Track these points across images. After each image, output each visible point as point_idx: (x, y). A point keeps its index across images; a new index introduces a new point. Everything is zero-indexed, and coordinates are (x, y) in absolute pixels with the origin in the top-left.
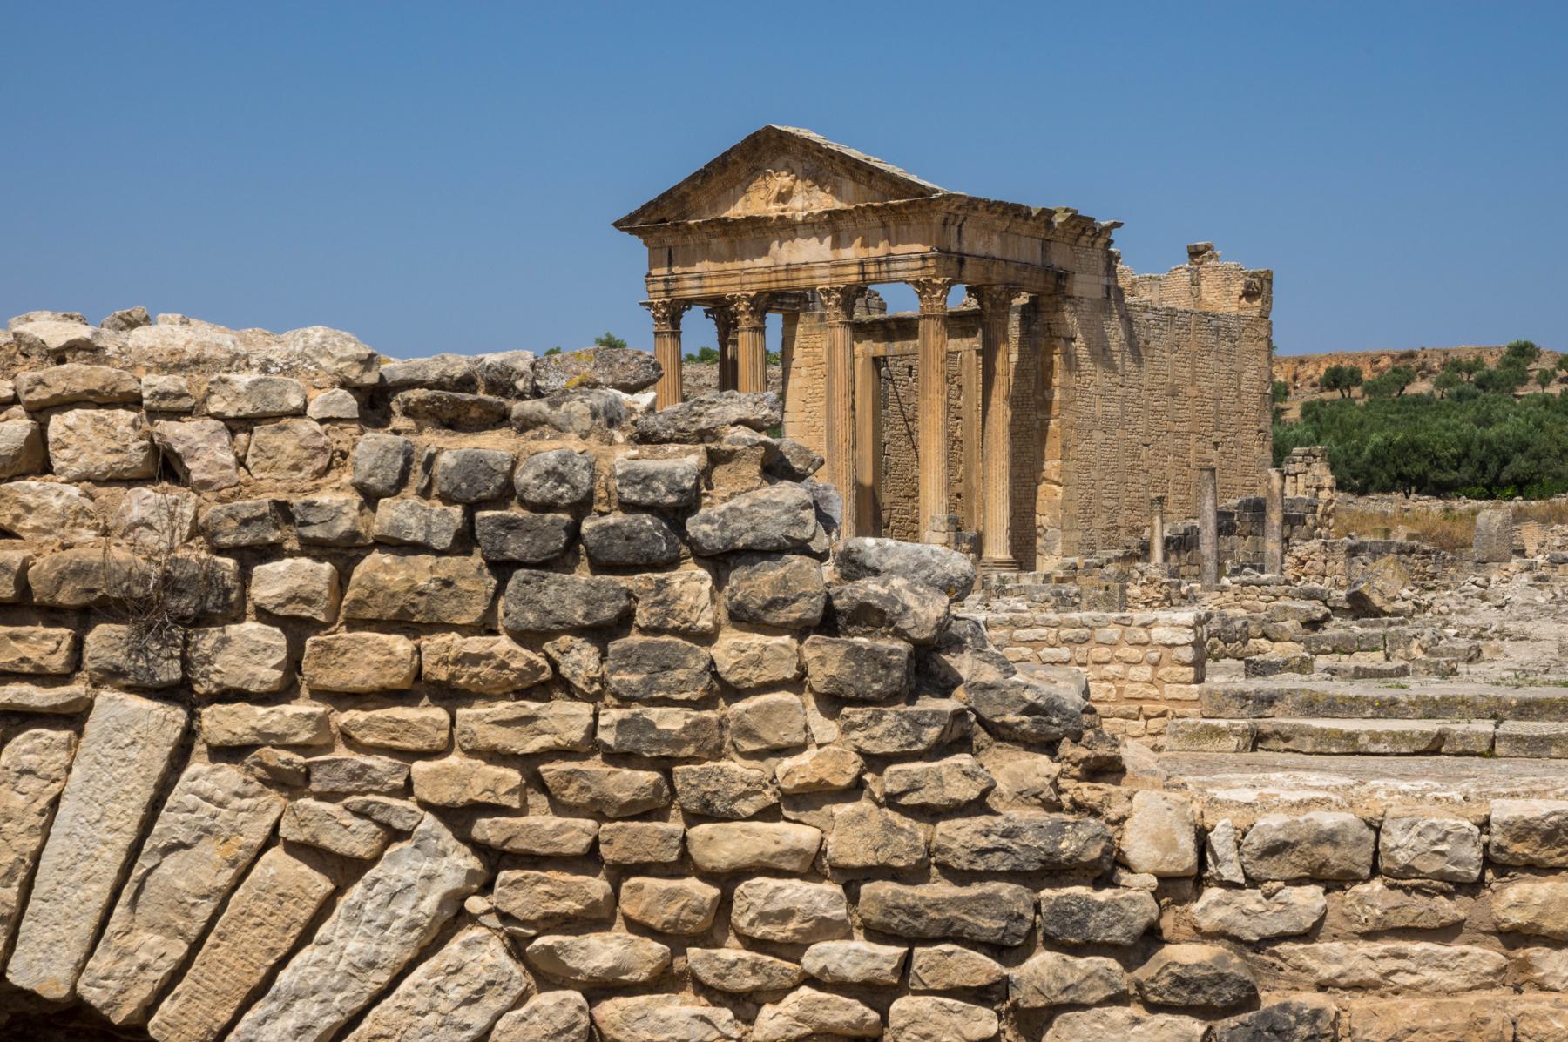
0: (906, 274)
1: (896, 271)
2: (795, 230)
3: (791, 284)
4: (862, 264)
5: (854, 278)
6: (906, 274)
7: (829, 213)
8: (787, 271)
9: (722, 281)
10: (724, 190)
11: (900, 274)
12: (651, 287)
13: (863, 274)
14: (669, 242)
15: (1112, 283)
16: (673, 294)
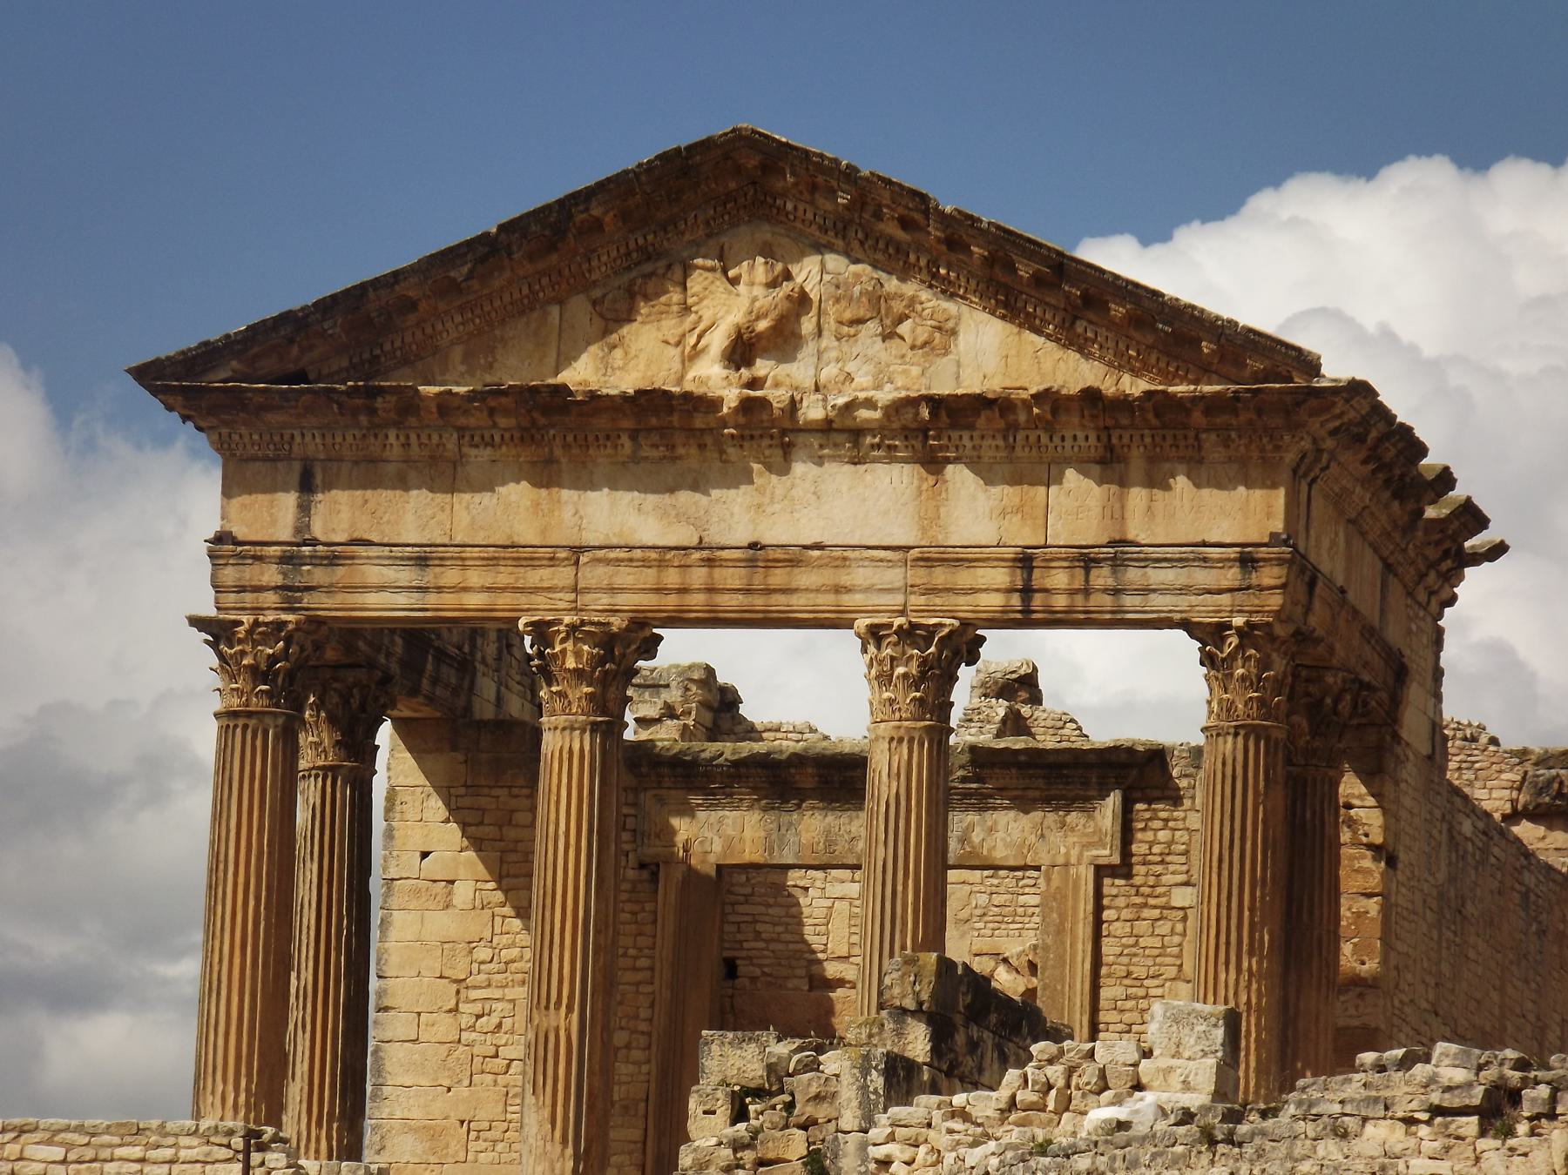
0: (1183, 602)
1: (1147, 591)
3: (758, 601)
4: (1025, 561)
5: (993, 601)
6: (1183, 602)
7: (935, 402)
8: (751, 563)
9: (504, 577)
10: (529, 305)
11: (1160, 603)
12: (230, 575)
13: (1027, 591)
14: (313, 445)
15: (1437, 720)
16: (308, 600)
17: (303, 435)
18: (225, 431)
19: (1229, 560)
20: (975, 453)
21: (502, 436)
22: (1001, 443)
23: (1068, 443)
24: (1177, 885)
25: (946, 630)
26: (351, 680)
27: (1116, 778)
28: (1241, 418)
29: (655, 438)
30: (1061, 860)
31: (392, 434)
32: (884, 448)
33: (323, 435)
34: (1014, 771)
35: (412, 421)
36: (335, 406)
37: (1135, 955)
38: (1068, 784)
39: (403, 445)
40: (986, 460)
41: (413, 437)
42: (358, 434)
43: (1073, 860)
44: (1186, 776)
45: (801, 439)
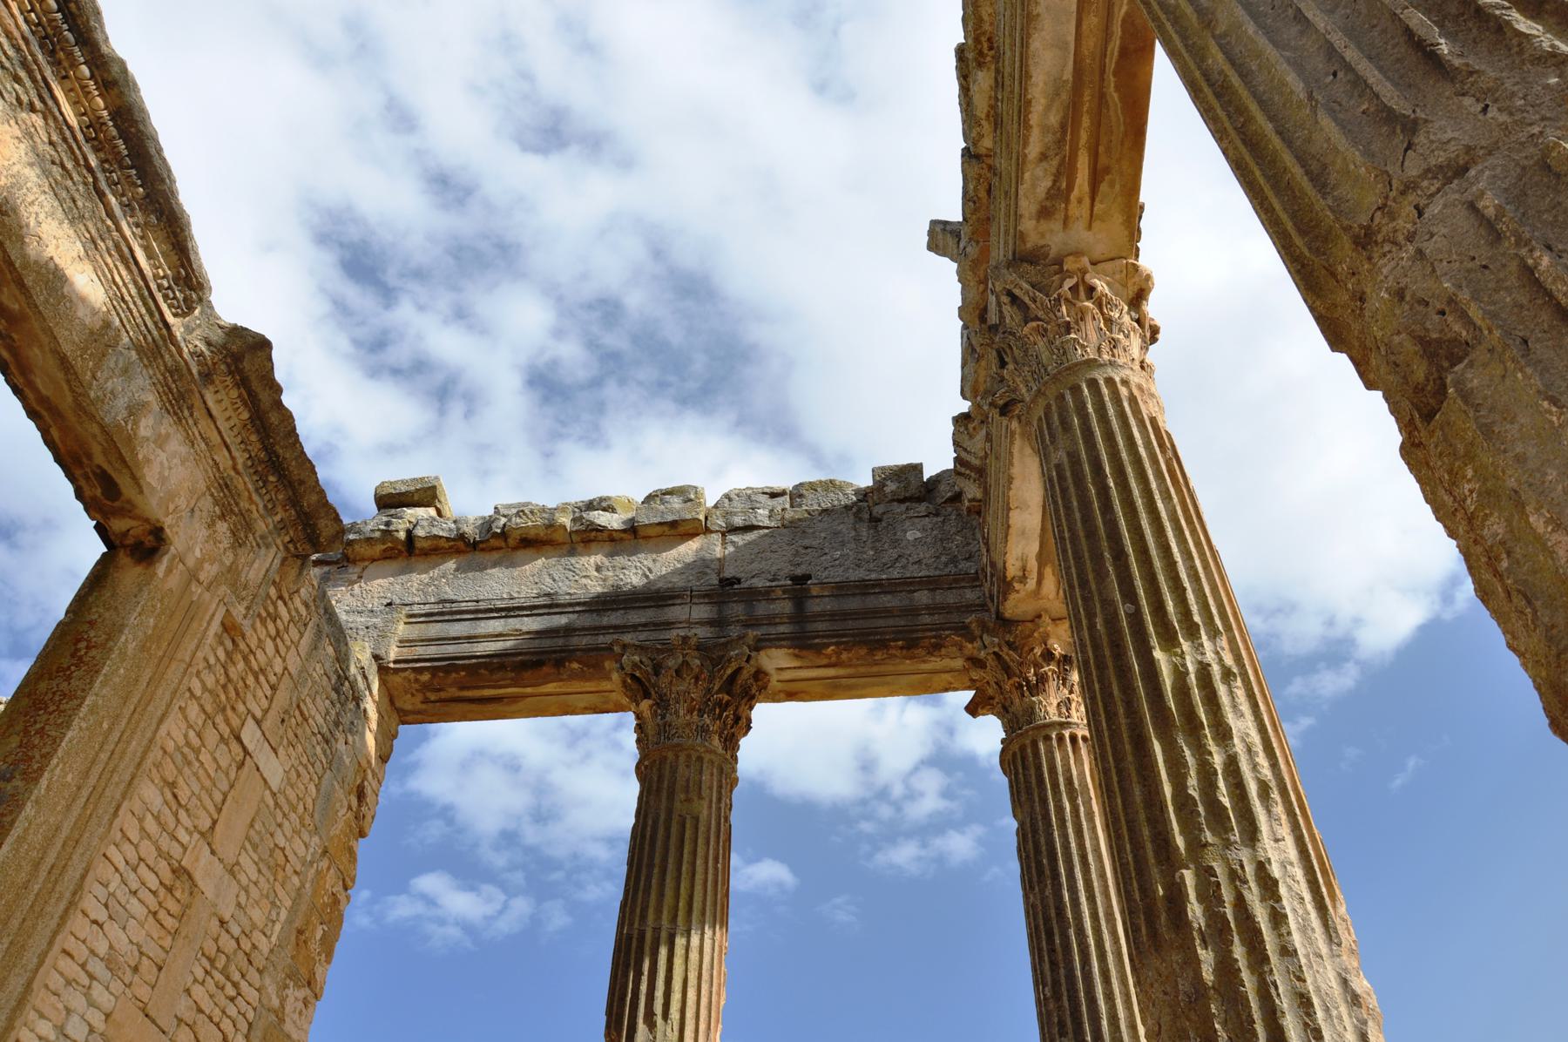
24: (254, 717)
30: (191, 562)
34: (246, 415)
37: (189, 764)
43: (202, 576)
44: (307, 605)
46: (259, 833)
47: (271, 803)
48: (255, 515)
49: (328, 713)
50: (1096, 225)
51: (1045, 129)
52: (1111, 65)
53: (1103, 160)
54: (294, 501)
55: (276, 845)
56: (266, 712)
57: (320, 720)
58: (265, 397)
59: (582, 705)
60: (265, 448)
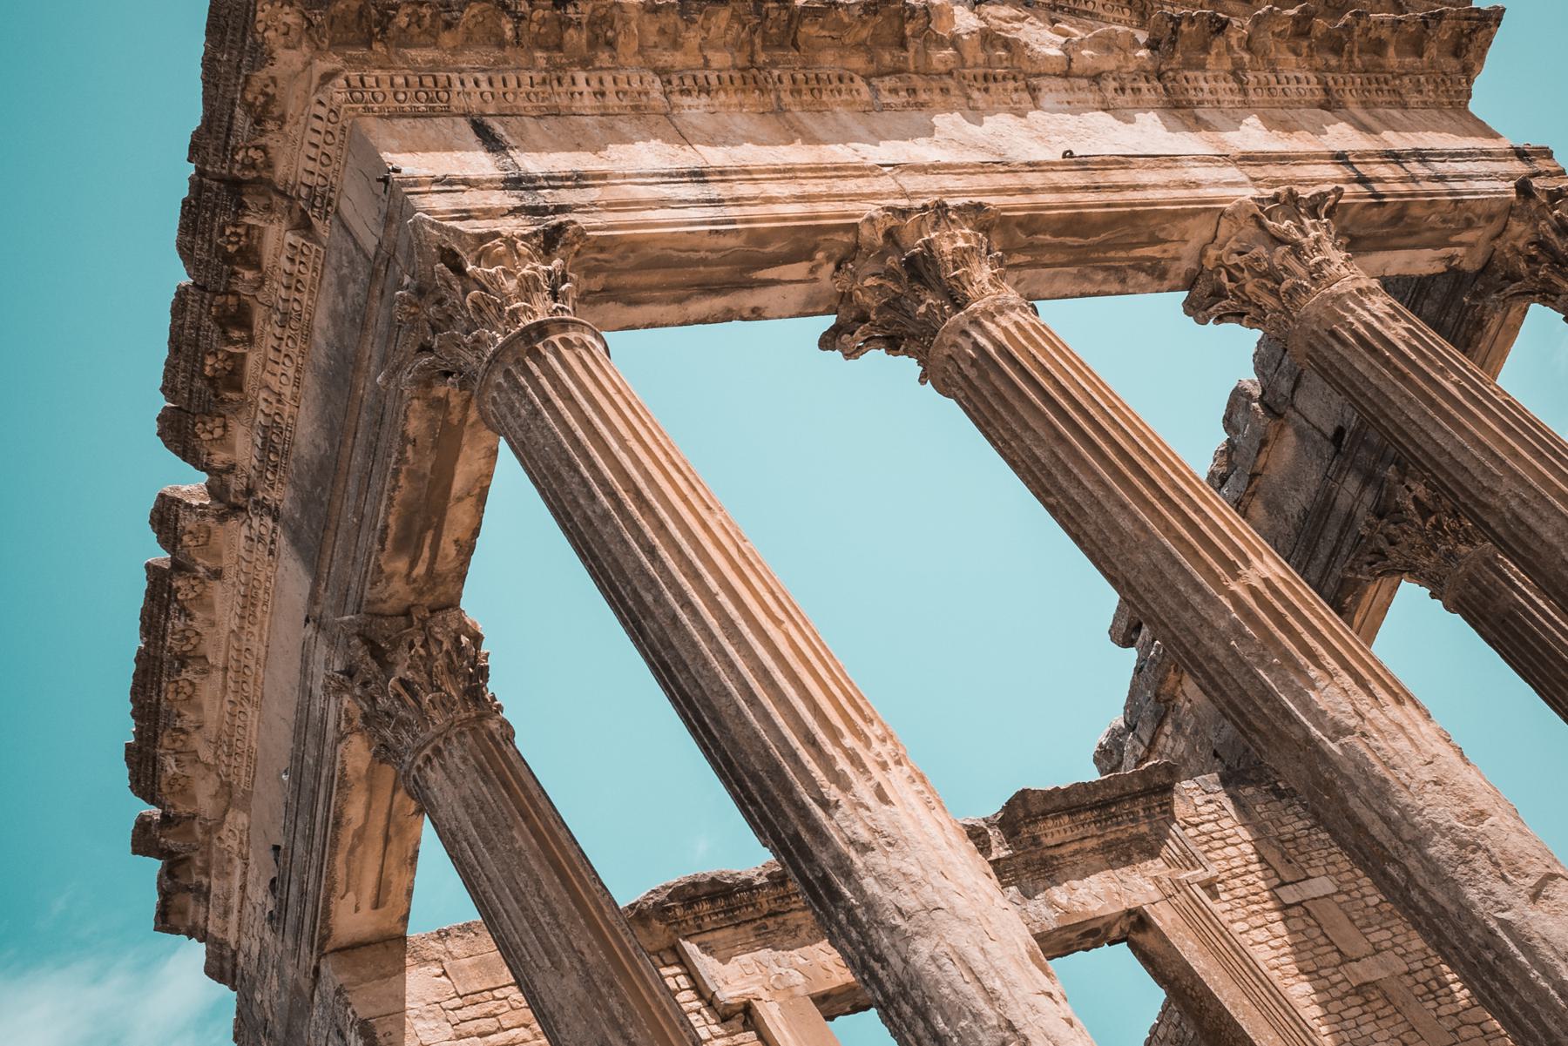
2: (1033, 91)
13: (1363, 180)
17: (462, 83)
18: (354, 76)
19: (1505, 154)
20: (1210, 97)
21: (718, 77)
22: (1235, 86)
23: (1293, 85)
24: (1278, 886)
25: (1333, 196)
26: (454, 625)
27: (1160, 806)
28: (1425, 59)
29: (889, 82)
31: (581, 76)
32: (1128, 91)
33: (491, 83)
34: (1066, 819)
35: (604, 57)
36: (508, 30)
38: (1118, 824)
39: (595, 94)
40: (1225, 105)
41: (608, 78)
42: (537, 79)
44: (1210, 802)
45: (1043, 82)
46: (1360, 918)
47: (1345, 897)
48: (1135, 831)
49: (1296, 814)
50: (1187, 237)
51: (1105, 281)
52: (1082, 241)
53: (1144, 238)
54: (1134, 797)
55: (1376, 906)
56: (1277, 875)
57: (1300, 825)
58: (1060, 801)
59: (1385, 597)
60: (1091, 809)
